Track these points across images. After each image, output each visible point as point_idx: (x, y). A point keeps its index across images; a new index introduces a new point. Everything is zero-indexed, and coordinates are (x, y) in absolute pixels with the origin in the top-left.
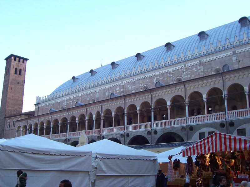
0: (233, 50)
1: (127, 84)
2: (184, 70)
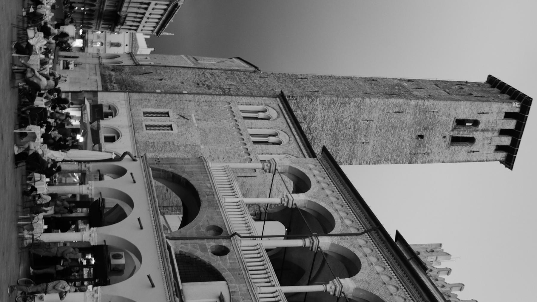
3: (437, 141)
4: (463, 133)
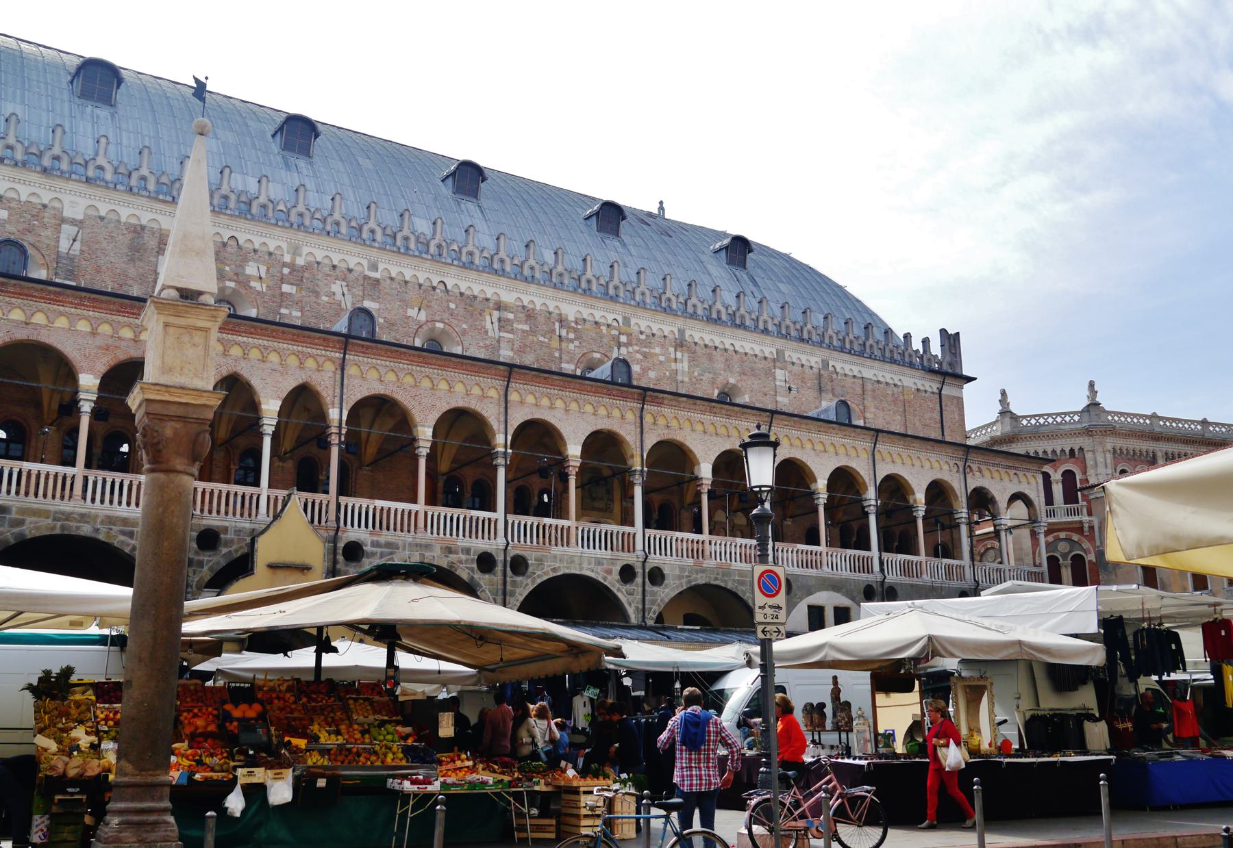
1: (327, 270)
2: (623, 339)
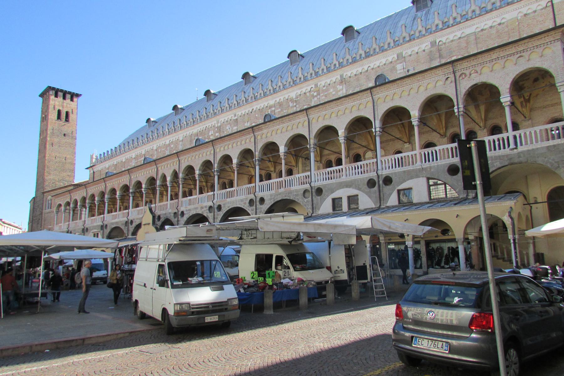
0: (398, 50)
1: (225, 123)
3: (67, 128)
4: (63, 116)
